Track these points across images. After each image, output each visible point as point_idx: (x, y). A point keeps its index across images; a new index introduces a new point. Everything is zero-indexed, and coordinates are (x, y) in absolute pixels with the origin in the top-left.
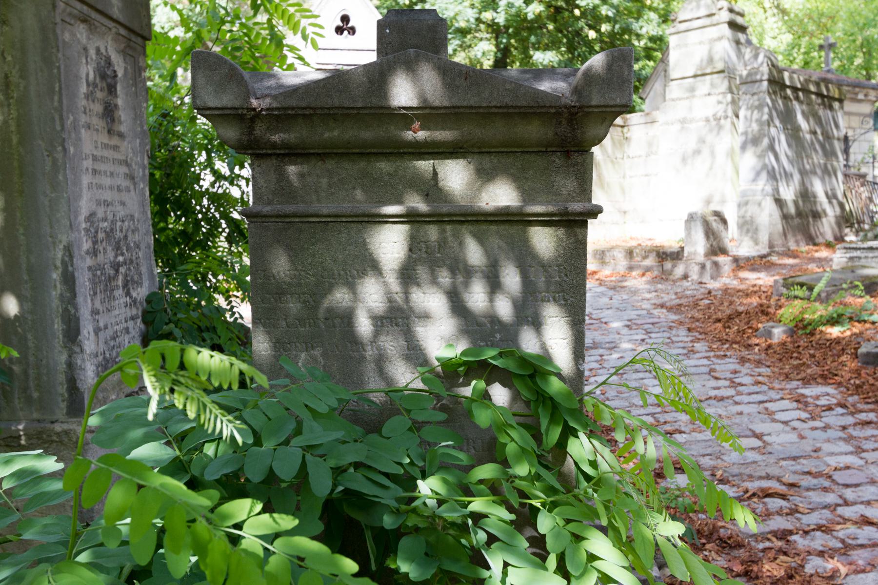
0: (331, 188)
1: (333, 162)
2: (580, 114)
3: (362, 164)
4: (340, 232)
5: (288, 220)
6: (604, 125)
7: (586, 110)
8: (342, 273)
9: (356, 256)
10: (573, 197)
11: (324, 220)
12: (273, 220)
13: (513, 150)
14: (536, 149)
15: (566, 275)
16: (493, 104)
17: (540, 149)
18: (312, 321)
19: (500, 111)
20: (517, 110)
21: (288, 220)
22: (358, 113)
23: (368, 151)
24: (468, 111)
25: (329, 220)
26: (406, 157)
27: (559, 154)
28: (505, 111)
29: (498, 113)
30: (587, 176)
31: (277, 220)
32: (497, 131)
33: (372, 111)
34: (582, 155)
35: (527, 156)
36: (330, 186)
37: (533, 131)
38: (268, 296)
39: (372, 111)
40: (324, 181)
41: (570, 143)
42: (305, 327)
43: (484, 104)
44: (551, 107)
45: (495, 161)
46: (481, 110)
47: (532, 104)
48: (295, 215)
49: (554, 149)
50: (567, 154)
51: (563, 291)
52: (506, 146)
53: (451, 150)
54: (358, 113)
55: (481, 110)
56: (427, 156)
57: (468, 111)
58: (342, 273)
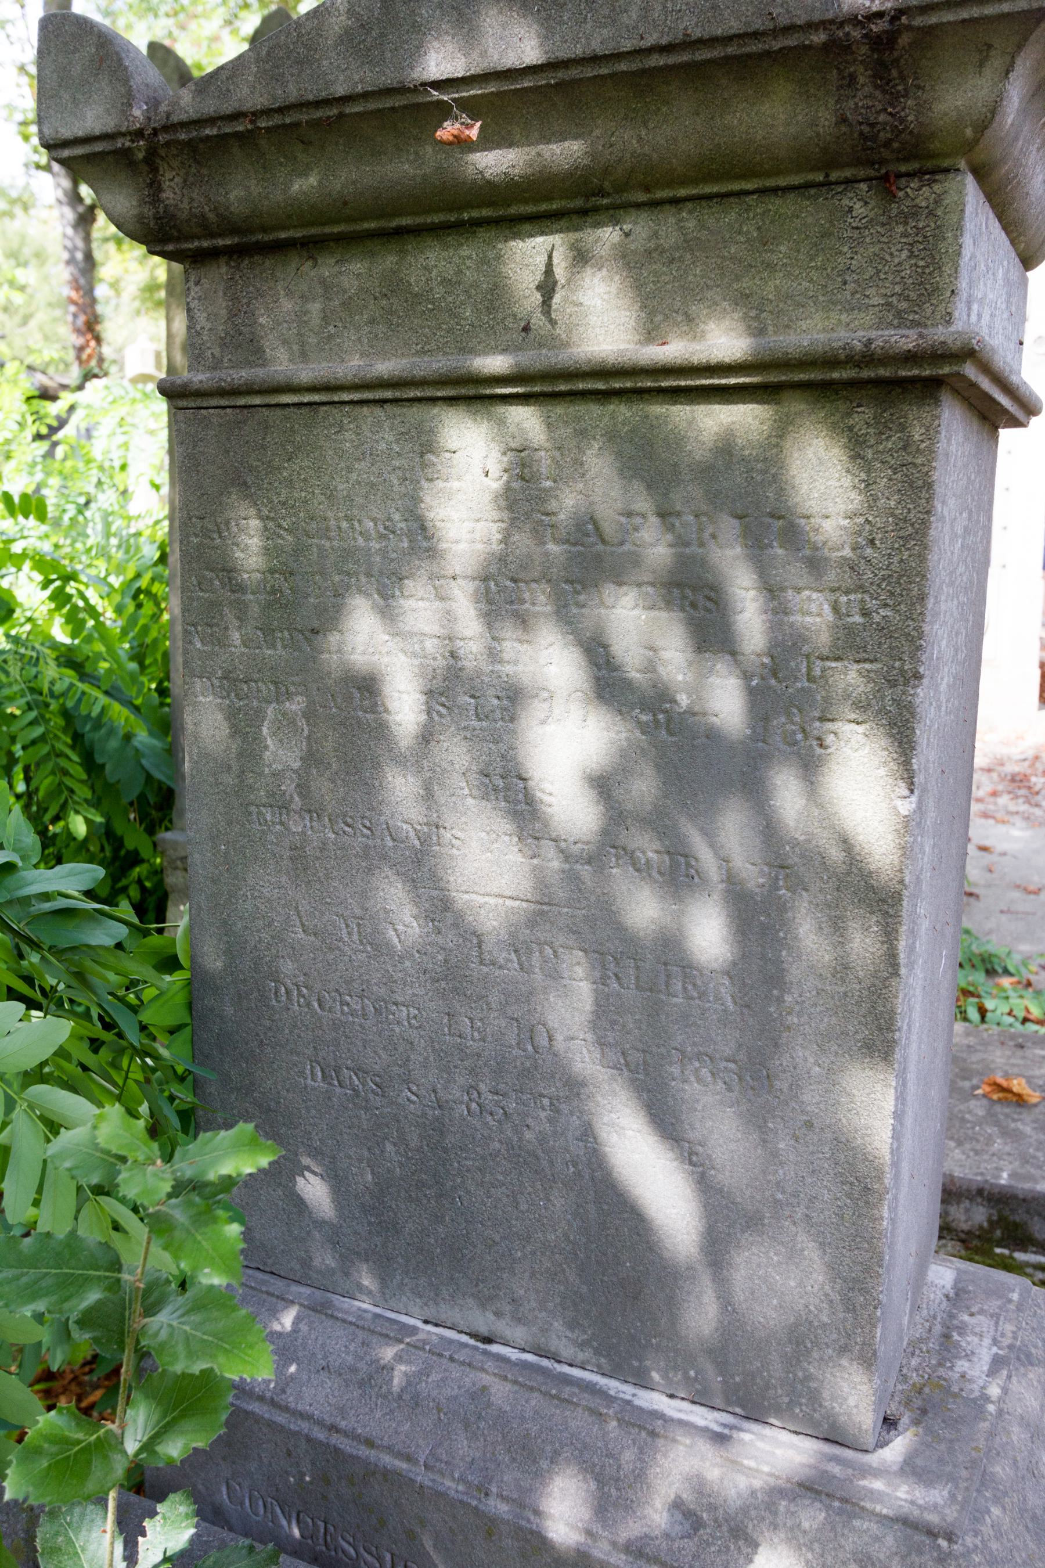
0: (328, 324)
1: (332, 261)
2: (904, 40)
3: (390, 260)
4: (341, 429)
5: (242, 401)
6: (987, 71)
7: (918, 21)
8: (345, 525)
9: (372, 485)
10: (899, 314)
11: (307, 398)
12: (214, 402)
13: (736, 186)
14: (796, 180)
15: (872, 542)
16: (650, 41)
17: (811, 177)
18: (286, 633)
19: (672, 59)
20: (716, 53)
21: (242, 401)
22: (341, 115)
23: (394, 223)
24: (589, 72)
25: (316, 398)
26: (482, 233)
27: (864, 186)
28: (685, 57)
29: (667, 68)
30: (942, 246)
31: (223, 402)
32: (675, 131)
33: (372, 106)
34: (931, 183)
35: (775, 204)
36: (325, 319)
37: (777, 117)
38: (209, 574)
39: (372, 106)
40: (315, 308)
41: (887, 144)
42: (273, 646)
43: (627, 46)
44: (811, 26)
45: (691, 224)
46: (623, 66)
47: (758, 25)
48: (249, 390)
49: (848, 173)
50: (886, 185)
51: (860, 588)
52: (709, 177)
53: (578, 203)
54: (341, 115)
55: (623, 66)
56: (527, 227)
57: (589, 72)
58: (345, 525)
